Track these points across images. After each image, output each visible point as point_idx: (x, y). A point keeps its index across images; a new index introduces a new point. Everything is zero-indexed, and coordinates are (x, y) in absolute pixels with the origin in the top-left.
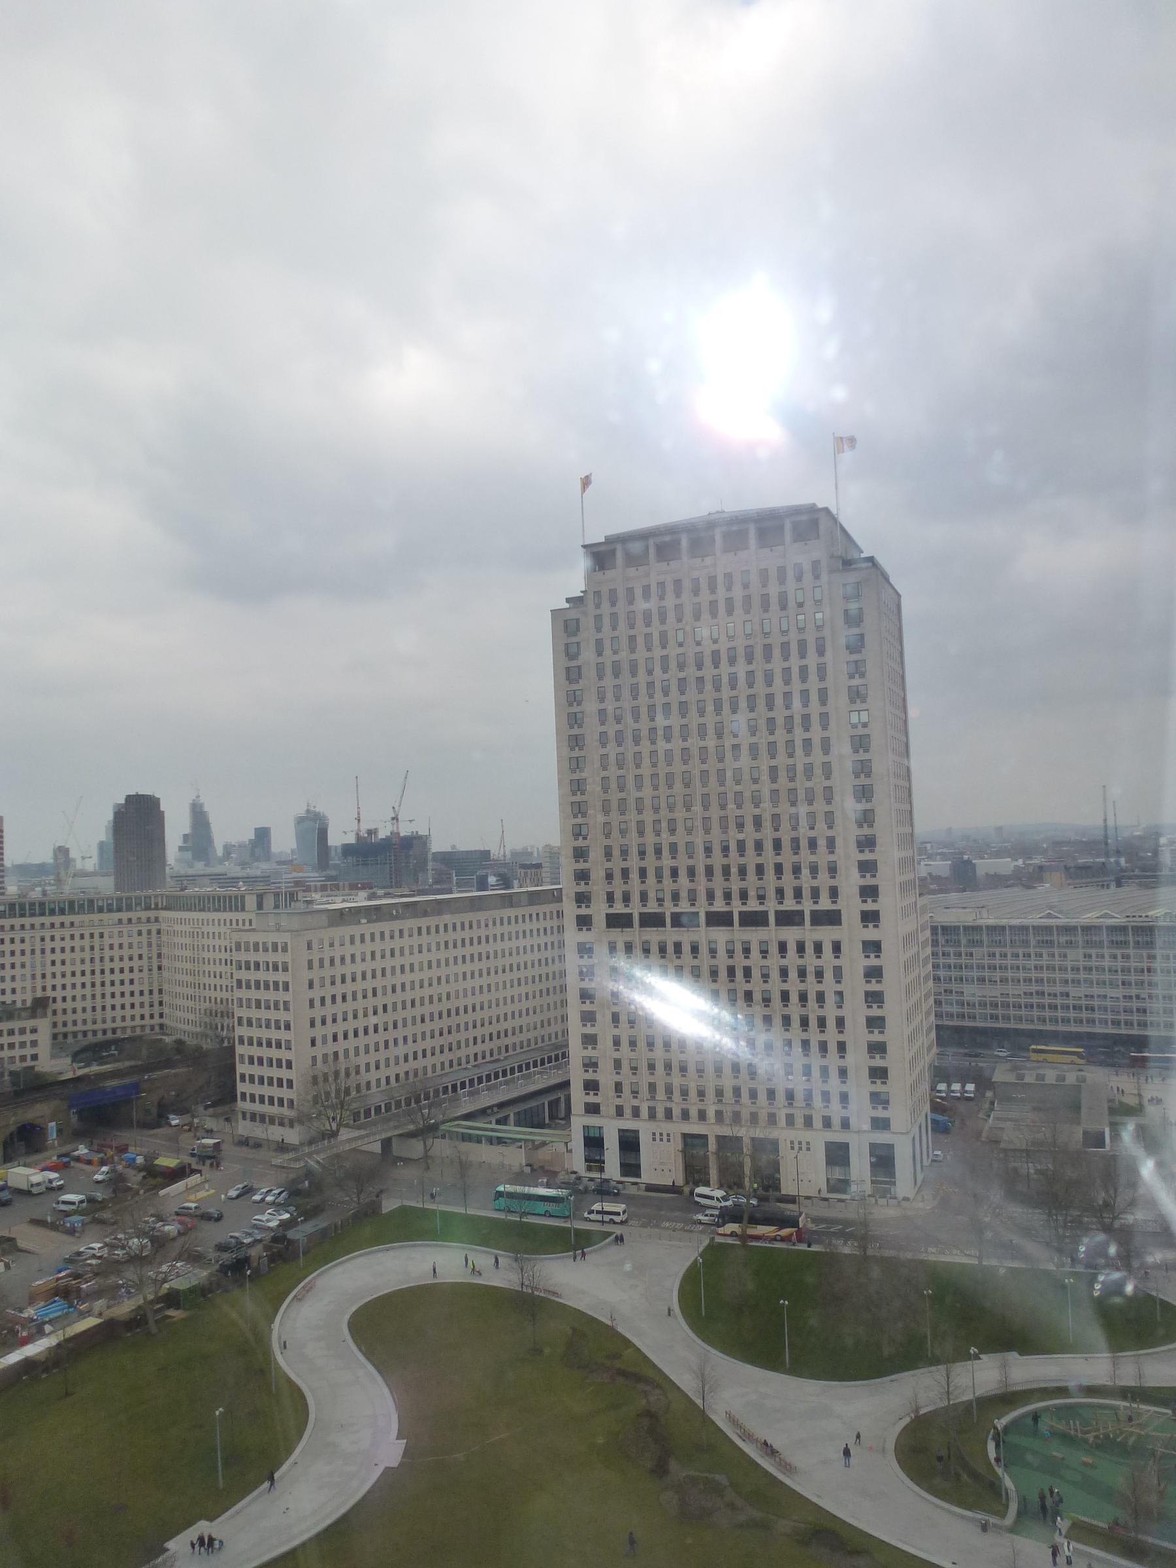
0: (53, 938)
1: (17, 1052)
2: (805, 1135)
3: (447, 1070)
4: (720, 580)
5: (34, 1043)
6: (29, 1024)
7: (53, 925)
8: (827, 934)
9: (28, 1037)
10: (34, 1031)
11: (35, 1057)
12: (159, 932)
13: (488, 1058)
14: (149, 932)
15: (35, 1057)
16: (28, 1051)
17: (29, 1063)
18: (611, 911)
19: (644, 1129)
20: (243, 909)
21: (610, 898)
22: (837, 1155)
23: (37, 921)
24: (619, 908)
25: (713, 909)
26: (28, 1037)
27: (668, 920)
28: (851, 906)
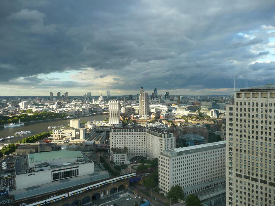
1: (121, 159)
3: (200, 183)
4: (268, 104)
5: (124, 158)
7: (128, 134)
9: (123, 157)
10: (124, 156)
13: (209, 181)
15: (124, 161)
16: (123, 159)
17: (123, 161)
18: (237, 173)
20: (161, 137)
21: (237, 170)
24: (239, 173)
25: (262, 179)
26: (123, 157)
27: (251, 179)
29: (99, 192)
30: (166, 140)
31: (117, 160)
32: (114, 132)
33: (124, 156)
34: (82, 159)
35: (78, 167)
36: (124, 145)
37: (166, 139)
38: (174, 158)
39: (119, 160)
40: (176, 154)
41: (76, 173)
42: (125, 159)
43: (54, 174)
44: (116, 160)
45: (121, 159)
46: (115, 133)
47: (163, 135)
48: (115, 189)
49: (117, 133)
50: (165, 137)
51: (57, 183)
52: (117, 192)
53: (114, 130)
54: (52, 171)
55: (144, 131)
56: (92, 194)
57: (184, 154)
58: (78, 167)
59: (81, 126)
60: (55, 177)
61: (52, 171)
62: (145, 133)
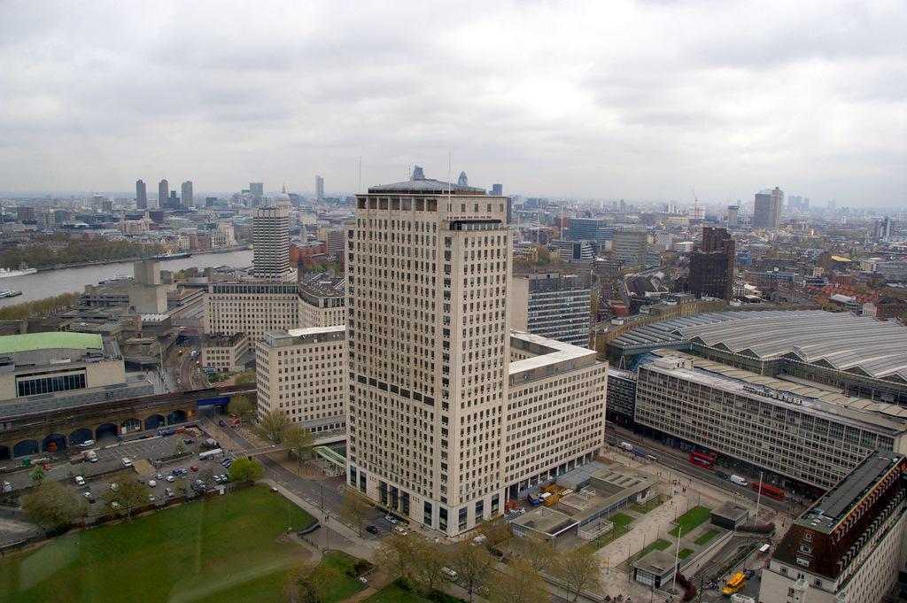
0: (249, 304)
1: (221, 361)
2: (418, 496)
5: (228, 358)
6: (225, 349)
7: (249, 298)
8: (429, 408)
11: (228, 364)
12: (297, 304)
14: (293, 304)
15: (228, 364)
16: (226, 361)
17: (226, 366)
19: (369, 474)
22: (428, 508)
23: (243, 295)
24: (362, 374)
26: (225, 355)
28: (439, 399)
29: (116, 420)
30: (326, 313)
31: (211, 361)
32: (215, 292)
33: (227, 352)
34: (99, 351)
35: (84, 368)
36: (241, 328)
37: (328, 310)
38: (282, 350)
39: (216, 361)
40: (290, 340)
41: (79, 382)
42: (232, 361)
43: (21, 385)
44: (209, 361)
45: (221, 361)
46: (217, 295)
47: (321, 302)
48: (161, 419)
49: (221, 295)
50: (326, 305)
51: (25, 400)
52: (164, 425)
53: (215, 287)
54: (17, 376)
55: (293, 292)
56: (96, 424)
57: (316, 341)
58: (84, 368)
59: (162, 278)
60: (24, 389)
61: (17, 376)
62: (295, 295)
